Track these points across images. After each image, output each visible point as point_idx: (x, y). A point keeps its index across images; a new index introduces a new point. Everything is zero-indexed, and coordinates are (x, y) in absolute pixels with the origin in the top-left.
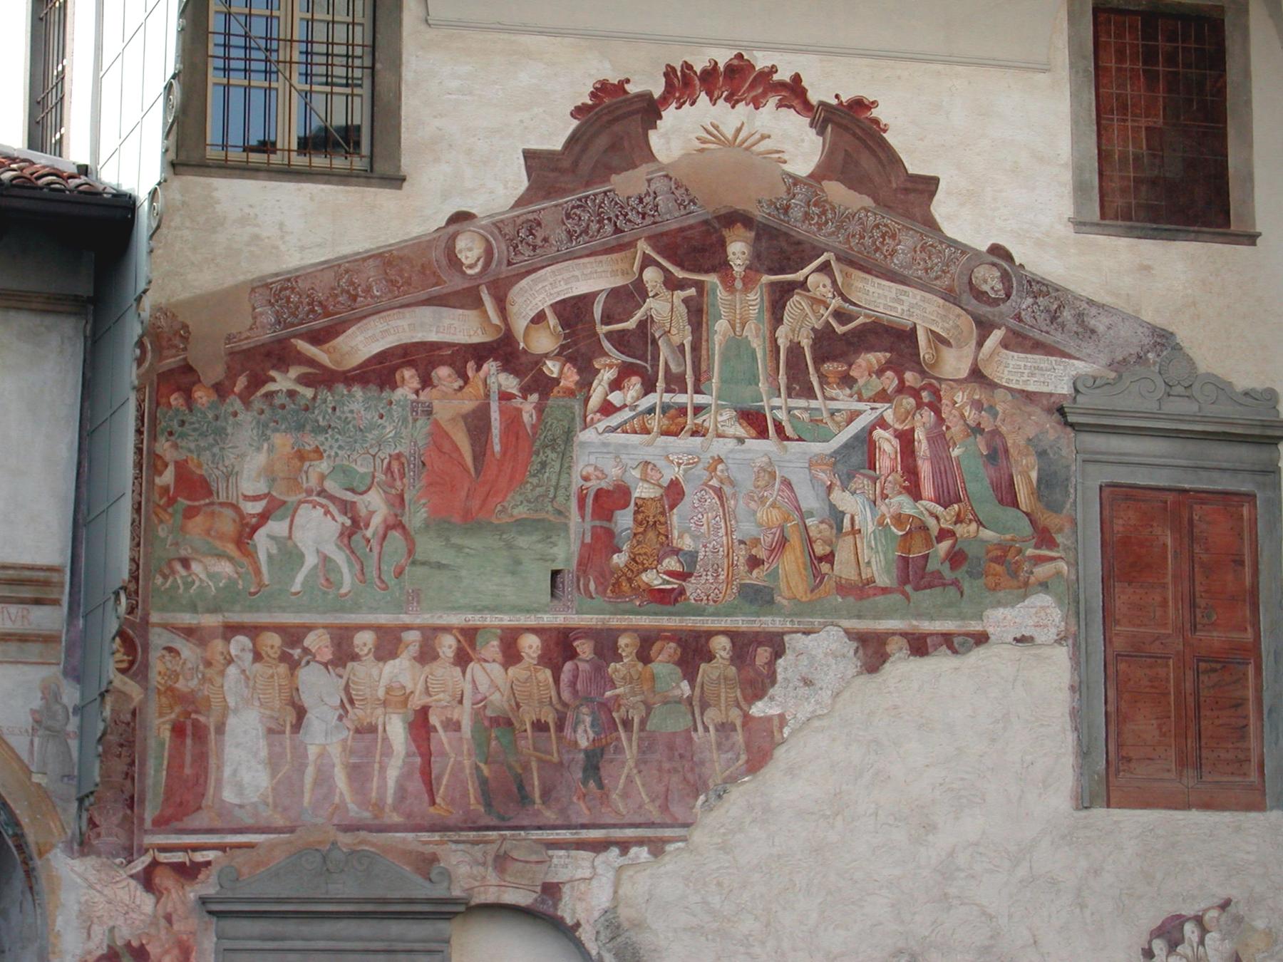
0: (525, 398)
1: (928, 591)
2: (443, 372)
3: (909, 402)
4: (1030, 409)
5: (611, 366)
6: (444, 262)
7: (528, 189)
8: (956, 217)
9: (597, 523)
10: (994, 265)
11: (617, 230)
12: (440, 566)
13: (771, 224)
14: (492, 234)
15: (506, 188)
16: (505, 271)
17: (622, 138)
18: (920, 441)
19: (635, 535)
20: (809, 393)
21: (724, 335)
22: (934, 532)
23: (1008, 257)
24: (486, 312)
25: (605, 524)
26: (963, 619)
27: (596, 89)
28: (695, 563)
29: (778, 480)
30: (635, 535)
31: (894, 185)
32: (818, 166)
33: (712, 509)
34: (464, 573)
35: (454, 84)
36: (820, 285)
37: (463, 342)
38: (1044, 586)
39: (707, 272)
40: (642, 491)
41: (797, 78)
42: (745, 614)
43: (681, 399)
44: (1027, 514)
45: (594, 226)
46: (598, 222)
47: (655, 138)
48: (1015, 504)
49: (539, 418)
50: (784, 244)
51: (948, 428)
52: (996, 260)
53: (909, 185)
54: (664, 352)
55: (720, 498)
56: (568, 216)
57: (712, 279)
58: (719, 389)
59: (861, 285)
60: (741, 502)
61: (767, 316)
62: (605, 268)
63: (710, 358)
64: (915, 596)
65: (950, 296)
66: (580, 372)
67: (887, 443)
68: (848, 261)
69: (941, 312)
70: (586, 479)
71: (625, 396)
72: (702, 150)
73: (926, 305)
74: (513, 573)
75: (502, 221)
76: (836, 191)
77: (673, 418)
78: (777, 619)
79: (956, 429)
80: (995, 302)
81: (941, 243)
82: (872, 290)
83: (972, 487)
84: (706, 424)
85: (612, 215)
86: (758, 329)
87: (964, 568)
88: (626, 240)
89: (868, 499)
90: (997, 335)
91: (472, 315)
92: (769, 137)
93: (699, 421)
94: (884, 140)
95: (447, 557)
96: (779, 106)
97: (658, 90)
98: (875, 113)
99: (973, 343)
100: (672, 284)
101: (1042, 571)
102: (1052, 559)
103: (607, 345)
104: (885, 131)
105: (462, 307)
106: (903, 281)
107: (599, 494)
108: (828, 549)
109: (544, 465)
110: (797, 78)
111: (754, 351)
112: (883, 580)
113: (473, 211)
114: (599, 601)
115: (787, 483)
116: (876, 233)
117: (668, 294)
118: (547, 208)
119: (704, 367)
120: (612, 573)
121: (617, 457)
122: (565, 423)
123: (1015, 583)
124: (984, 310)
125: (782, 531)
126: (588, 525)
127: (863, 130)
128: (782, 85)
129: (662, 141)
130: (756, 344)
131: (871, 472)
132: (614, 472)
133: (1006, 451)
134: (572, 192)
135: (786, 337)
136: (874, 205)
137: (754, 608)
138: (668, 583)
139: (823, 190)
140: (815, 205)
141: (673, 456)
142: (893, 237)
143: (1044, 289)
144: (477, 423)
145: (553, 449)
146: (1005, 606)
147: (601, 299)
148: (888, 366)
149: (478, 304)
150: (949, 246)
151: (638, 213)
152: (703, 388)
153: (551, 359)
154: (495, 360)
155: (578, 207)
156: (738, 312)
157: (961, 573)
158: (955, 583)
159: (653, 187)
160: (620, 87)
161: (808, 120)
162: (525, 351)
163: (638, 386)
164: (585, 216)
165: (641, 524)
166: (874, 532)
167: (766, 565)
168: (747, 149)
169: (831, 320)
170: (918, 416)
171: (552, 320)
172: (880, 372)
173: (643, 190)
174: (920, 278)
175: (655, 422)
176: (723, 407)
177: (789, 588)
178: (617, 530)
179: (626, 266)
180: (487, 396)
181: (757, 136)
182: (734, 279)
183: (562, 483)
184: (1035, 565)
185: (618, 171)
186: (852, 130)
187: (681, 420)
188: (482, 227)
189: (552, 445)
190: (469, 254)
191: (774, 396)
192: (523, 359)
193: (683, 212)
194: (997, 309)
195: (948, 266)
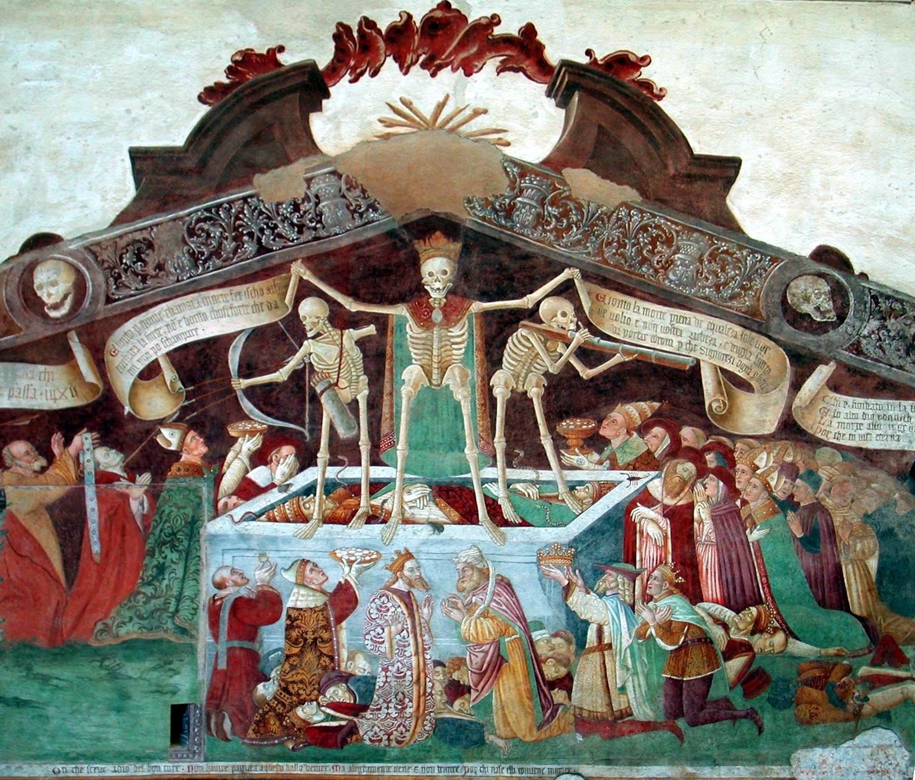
0: (132, 480)
1: (710, 726)
2: (19, 448)
3: (687, 468)
4: (870, 473)
5: (252, 433)
6: (18, 302)
7: (135, 200)
8: (762, 211)
9: (236, 644)
10: (821, 275)
11: (262, 249)
12: (19, 703)
13: (487, 232)
14: (84, 261)
15: (104, 199)
16: (103, 310)
17: (271, 126)
18: (701, 522)
19: (288, 657)
20: (541, 462)
21: (415, 386)
22: (721, 643)
23: (840, 261)
24: (76, 367)
25: (247, 644)
26: (762, 763)
27: (236, 62)
28: (372, 692)
29: (492, 581)
30: (288, 657)
31: (672, 171)
32: (558, 149)
33: (395, 620)
34: (51, 711)
35: (34, 66)
36: (557, 312)
37: (46, 407)
38: (884, 717)
39: (392, 302)
40: (297, 599)
41: (529, 31)
42: (442, 759)
43: (352, 473)
44: (861, 619)
45: (229, 245)
46: (235, 239)
47: (318, 124)
48: (843, 604)
49: (152, 505)
50: (506, 261)
51: (744, 503)
52: (823, 269)
53: (695, 170)
54: (329, 412)
55: (409, 606)
56: (191, 233)
57: (400, 311)
58: (406, 459)
59: (618, 311)
60: (438, 611)
61: (477, 357)
62: (244, 301)
63: (394, 416)
64: (691, 733)
65: (752, 322)
66: (208, 441)
67: (652, 526)
68: (600, 278)
69: (739, 343)
70: (220, 586)
71: (273, 472)
72: (386, 137)
73: (716, 335)
74: (119, 710)
75: (98, 244)
76: (584, 183)
77: (340, 500)
78: (490, 765)
79: (756, 503)
80: (822, 328)
81: (741, 248)
82: (634, 317)
83: (777, 582)
84: (387, 506)
85: (254, 229)
86: (464, 376)
87: (765, 695)
88: (275, 262)
89: (623, 602)
90: (823, 372)
91: (57, 374)
92: (485, 112)
93: (377, 502)
94: (658, 110)
95: (28, 691)
96: (501, 70)
97: (324, 58)
98: (646, 73)
99: (786, 385)
100: (340, 320)
101: (881, 697)
102: (898, 680)
103: (247, 405)
104: (660, 98)
105: (44, 362)
106: (683, 303)
107: (239, 604)
108: (563, 671)
109: (161, 569)
110: (529, 31)
111: (457, 406)
112: (643, 712)
113: (59, 232)
114: (236, 744)
115: (506, 584)
116: (643, 239)
117: (335, 333)
118: (161, 224)
119: (385, 429)
120: (256, 708)
121: (262, 555)
122: (189, 511)
123: (841, 714)
124: (805, 339)
125: (498, 648)
126: (223, 647)
127: (627, 96)
128: (507, 41)
129: (330, 126)
130: (461, 395)
131: (629, 567)
132: (258, 576)
133: (832, 533)
134: (198, 199)
135: (506, 385)
136: (639, 199)
137: (455, 750)
138: (334, 718)
139: (564, 183)
140: (552, 204)
141: (339, 550)
142: (669, 242)
143: (897, 306)
144: (68, 516)
145: (173, 548)
146: (824, 744)
147: (238, 344)
148: (657, 419)
149: (66, 356)
150: (753, 252)
151: (292, 225)
152: (383, 457)
153: (169, 426)
154: (90, 430)
155: (205, 220)
156: (436, 354)
157: (759, 702)
158: (751, 715)
159: (314, 188)
160: (270, 58)
161: (545, 87)
162: (131, 417)
163: (291, 459)
164: (217, 232)
165: (296, 642)
166: (631, 647)
167: (474, 694)
168: (452, 130)
169: (573, 361)
170: (699, 487)
171: (169, 374)
172: (644, 429)
173: (300, 192)
174: (706, 298)
175: (314, 506)
176: (412, 482)
177: (507, 723)
178: (262, 652)
179: (274, 297)
180: (81, 479)
181: (468, 112)
182: (431, 309)
183: (187, 593)
184: (872, 688)
185: (264, 168)
186: (612, 101)
187: (352, 501)
188: (71, 253)
189: (171, 541)
190: (53, 290)
191: (486, 464)
192: (130, 428)
193: (358, 222)
194: (823, 337)
195: (750, 279)
